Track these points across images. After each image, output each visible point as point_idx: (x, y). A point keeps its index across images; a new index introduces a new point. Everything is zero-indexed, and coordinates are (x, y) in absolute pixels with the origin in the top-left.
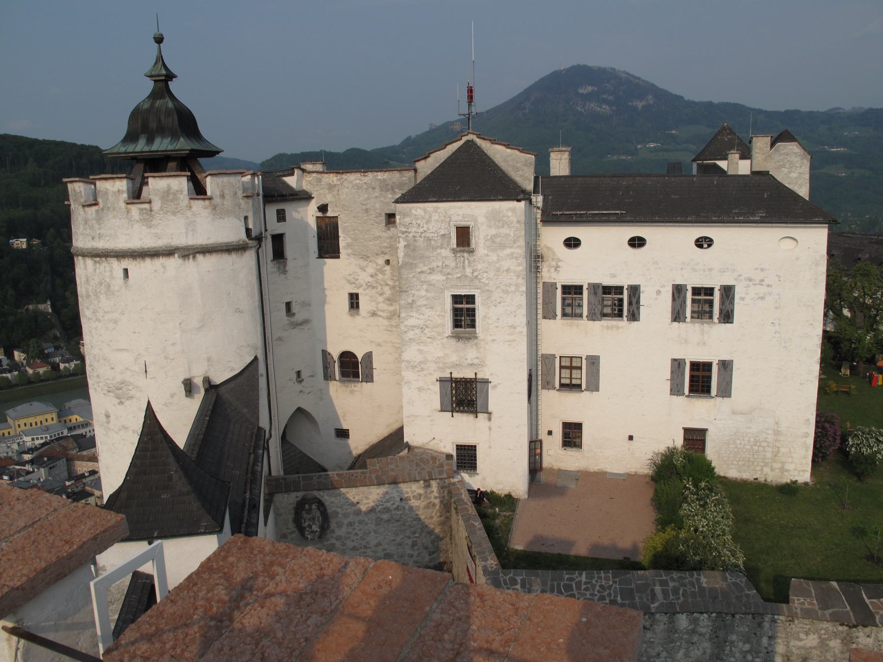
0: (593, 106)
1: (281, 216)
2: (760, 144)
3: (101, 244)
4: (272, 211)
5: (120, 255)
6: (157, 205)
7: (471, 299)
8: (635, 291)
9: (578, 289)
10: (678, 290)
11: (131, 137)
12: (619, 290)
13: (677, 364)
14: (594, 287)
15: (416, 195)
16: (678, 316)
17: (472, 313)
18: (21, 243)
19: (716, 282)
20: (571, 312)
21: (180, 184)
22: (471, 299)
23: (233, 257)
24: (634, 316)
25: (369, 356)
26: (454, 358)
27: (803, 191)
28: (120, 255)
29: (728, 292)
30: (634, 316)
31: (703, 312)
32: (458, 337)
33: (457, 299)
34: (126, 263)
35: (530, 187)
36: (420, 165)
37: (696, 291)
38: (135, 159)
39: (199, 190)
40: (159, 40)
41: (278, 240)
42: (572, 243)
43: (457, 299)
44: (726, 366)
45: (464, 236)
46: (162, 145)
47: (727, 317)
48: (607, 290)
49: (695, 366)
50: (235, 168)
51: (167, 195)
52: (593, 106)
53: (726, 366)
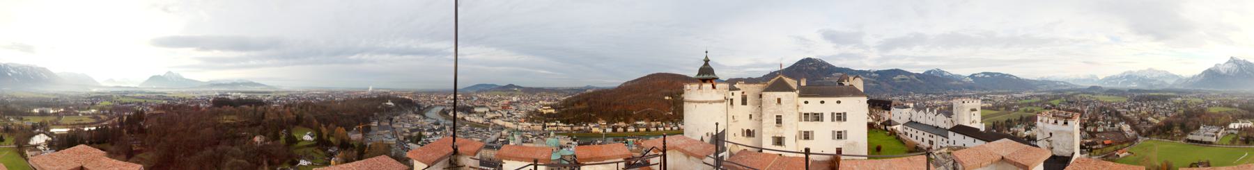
0: (813, 68)
1: (733, 94)
2: (851, 78)
3: (691, 99)
4: (731, 92)
5: (694, 102)
6: (704, 90)
7: (781, 116)
8: (822, 114)
9: (808, 114)
10: (833, 114)
11: (699, 74)
12: (818, 114)
13: (833, 132)
14: (812, 113)
15: (767, 90)
16: (833, 120)
17: (781, 120)
18: (667, 98)
19: (841, 112)
20: (806, 120)
21: (710, 85)
22: (781, 116)
23: (721, 104)
24: (822, 121)
25: (754, 131)
26: (776, 132)
27: (862, 90)
28: (694, 102)
29: (845, 114)
30: (822, 121)
31: (839, 119)
32: (778, 126)
33: (777, 116)
34: (696, 104)
35: (796, 88)
36: (768, 83)
37: (837, 114)
38: (700, 79)
39: (714, 87)
40: (707, 52)
41: (732, 100)
42: (806, 102)
43: (777, 116)
44: (845, 132)
45: (779, 101)
46: (706, 76)
47: (845, 120)
48: (815, 114)
49: (838, 132)
50: (722, 82)
51: (706, 88)
52: (813, 68)
53: (845, 132)
